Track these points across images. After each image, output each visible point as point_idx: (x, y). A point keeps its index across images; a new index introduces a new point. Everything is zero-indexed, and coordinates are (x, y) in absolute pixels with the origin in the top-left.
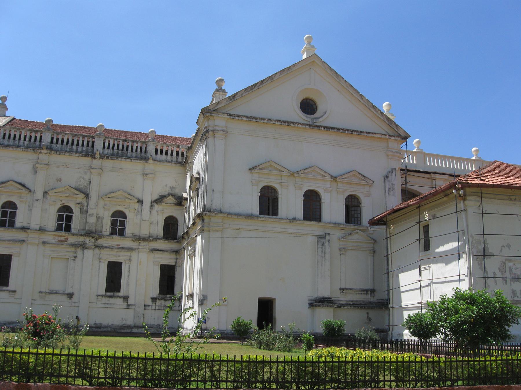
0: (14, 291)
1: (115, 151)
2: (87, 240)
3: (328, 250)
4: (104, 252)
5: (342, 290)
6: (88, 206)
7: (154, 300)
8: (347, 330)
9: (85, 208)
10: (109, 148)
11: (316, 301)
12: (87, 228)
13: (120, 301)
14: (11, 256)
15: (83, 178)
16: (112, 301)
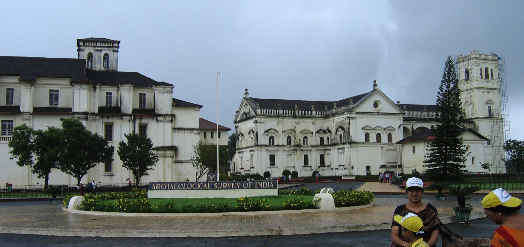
0: (277, 167)
1: (302, 114)
2: (297, 148)
3: (384, 151)
4: (302, 152)
5: (388, 162)
6: (296, 136)
7: (319, 167)
8: (347, 175)
9: (295, 136)
10: (300, 114)
11: (382, 166)
12: (297, 144)
13: (309, 168)
14: (274, 155)
15: (293, 126)
16: (307, 168)
